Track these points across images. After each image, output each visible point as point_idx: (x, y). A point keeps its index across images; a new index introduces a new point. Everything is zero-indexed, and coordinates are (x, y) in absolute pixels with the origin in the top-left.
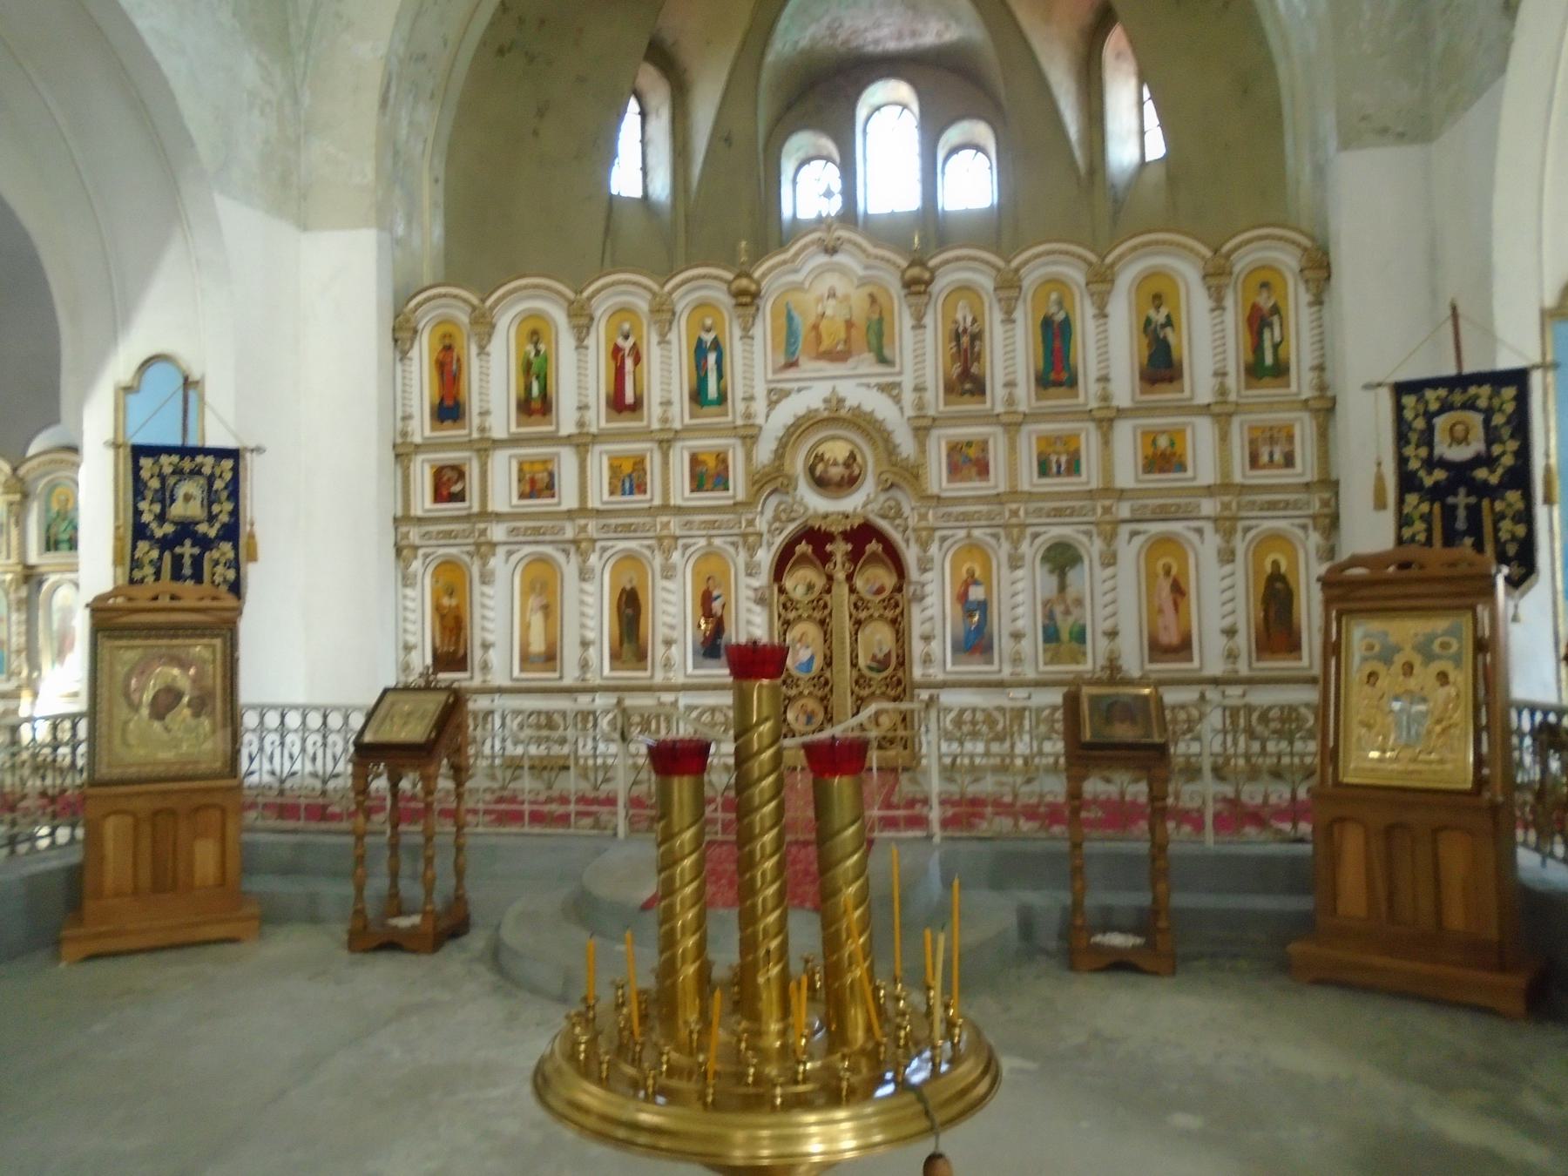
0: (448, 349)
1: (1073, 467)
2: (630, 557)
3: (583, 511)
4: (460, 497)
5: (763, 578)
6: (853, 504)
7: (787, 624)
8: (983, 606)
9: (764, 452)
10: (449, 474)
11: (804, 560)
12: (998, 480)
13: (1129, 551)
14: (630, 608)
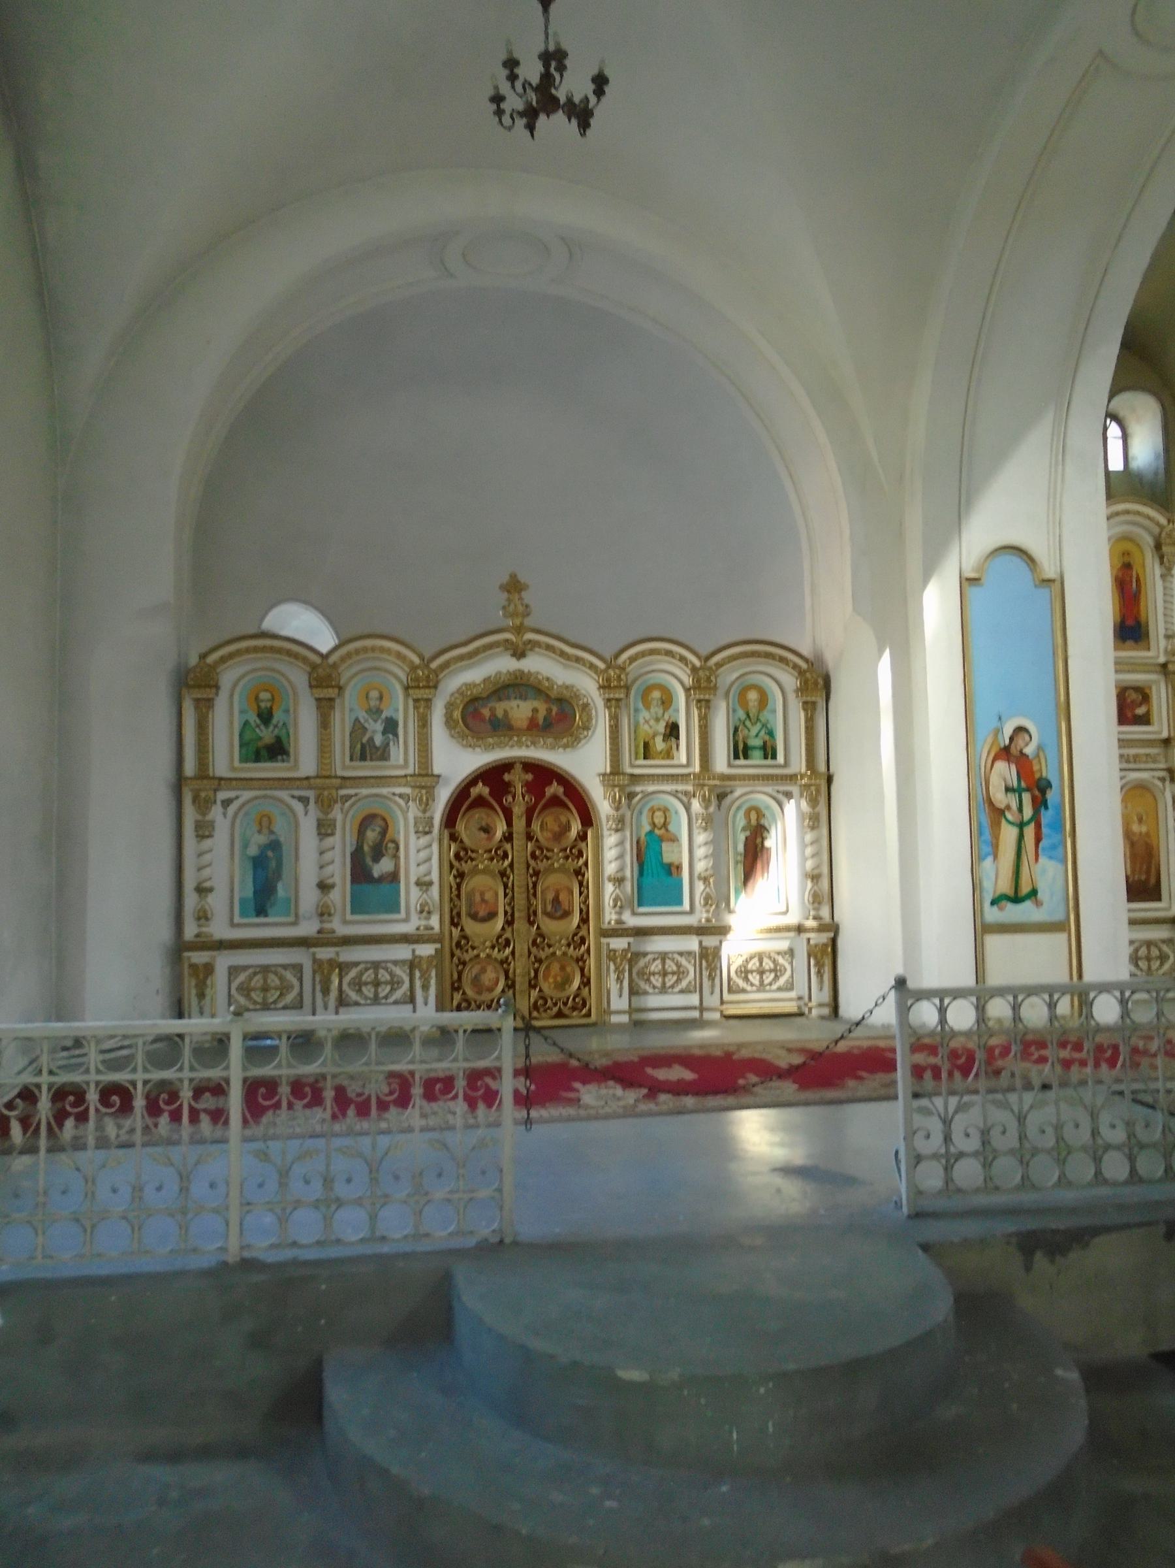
0: (1127, 566)
4: (1145, 720)
10: (1133, 696)
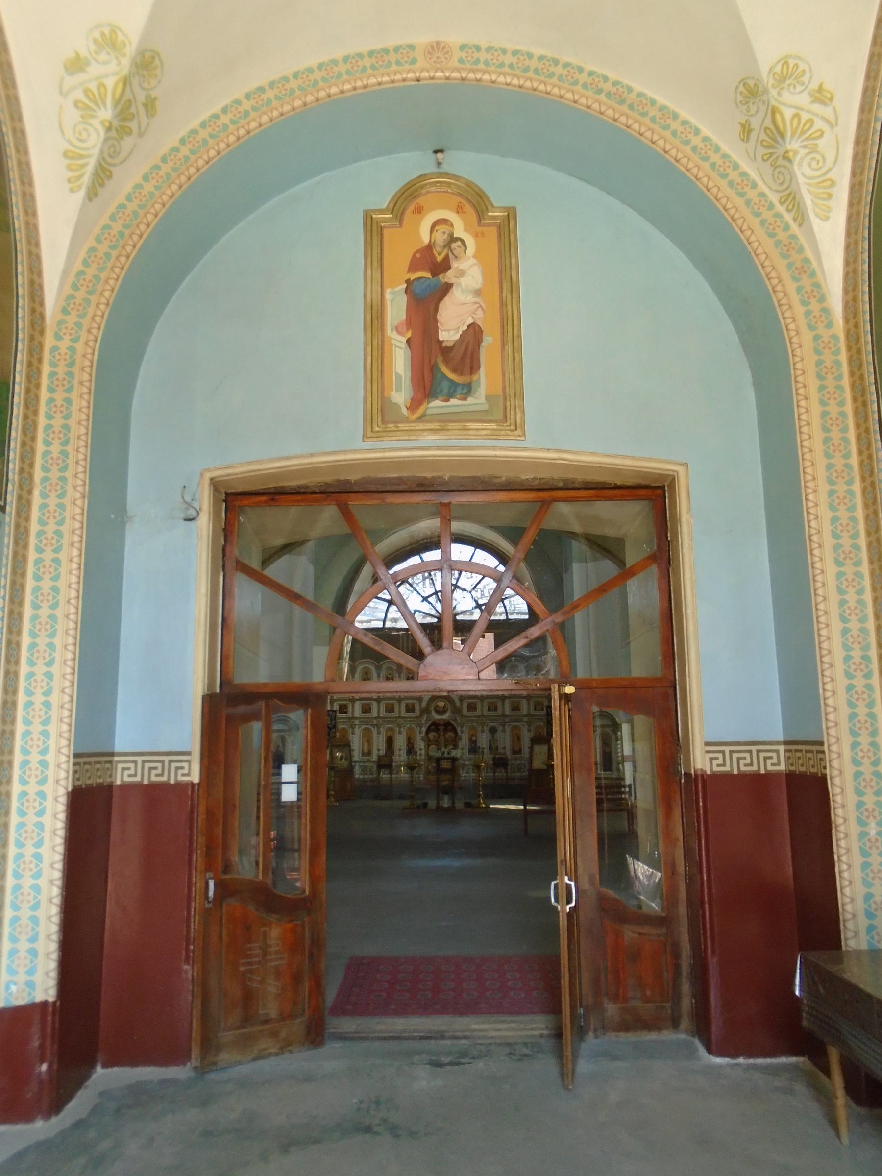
1: (496, 709)
2: (390, 729)
3: (378, 717)
4: (346, 713)
5: (423, 735)
6: (445, 717)
7: (429, 746)
8: (475, 742)
9: (424, 704)
11: (433, 730)
12: (479, 713)
13: (508, 729)
14: (390, 741)
